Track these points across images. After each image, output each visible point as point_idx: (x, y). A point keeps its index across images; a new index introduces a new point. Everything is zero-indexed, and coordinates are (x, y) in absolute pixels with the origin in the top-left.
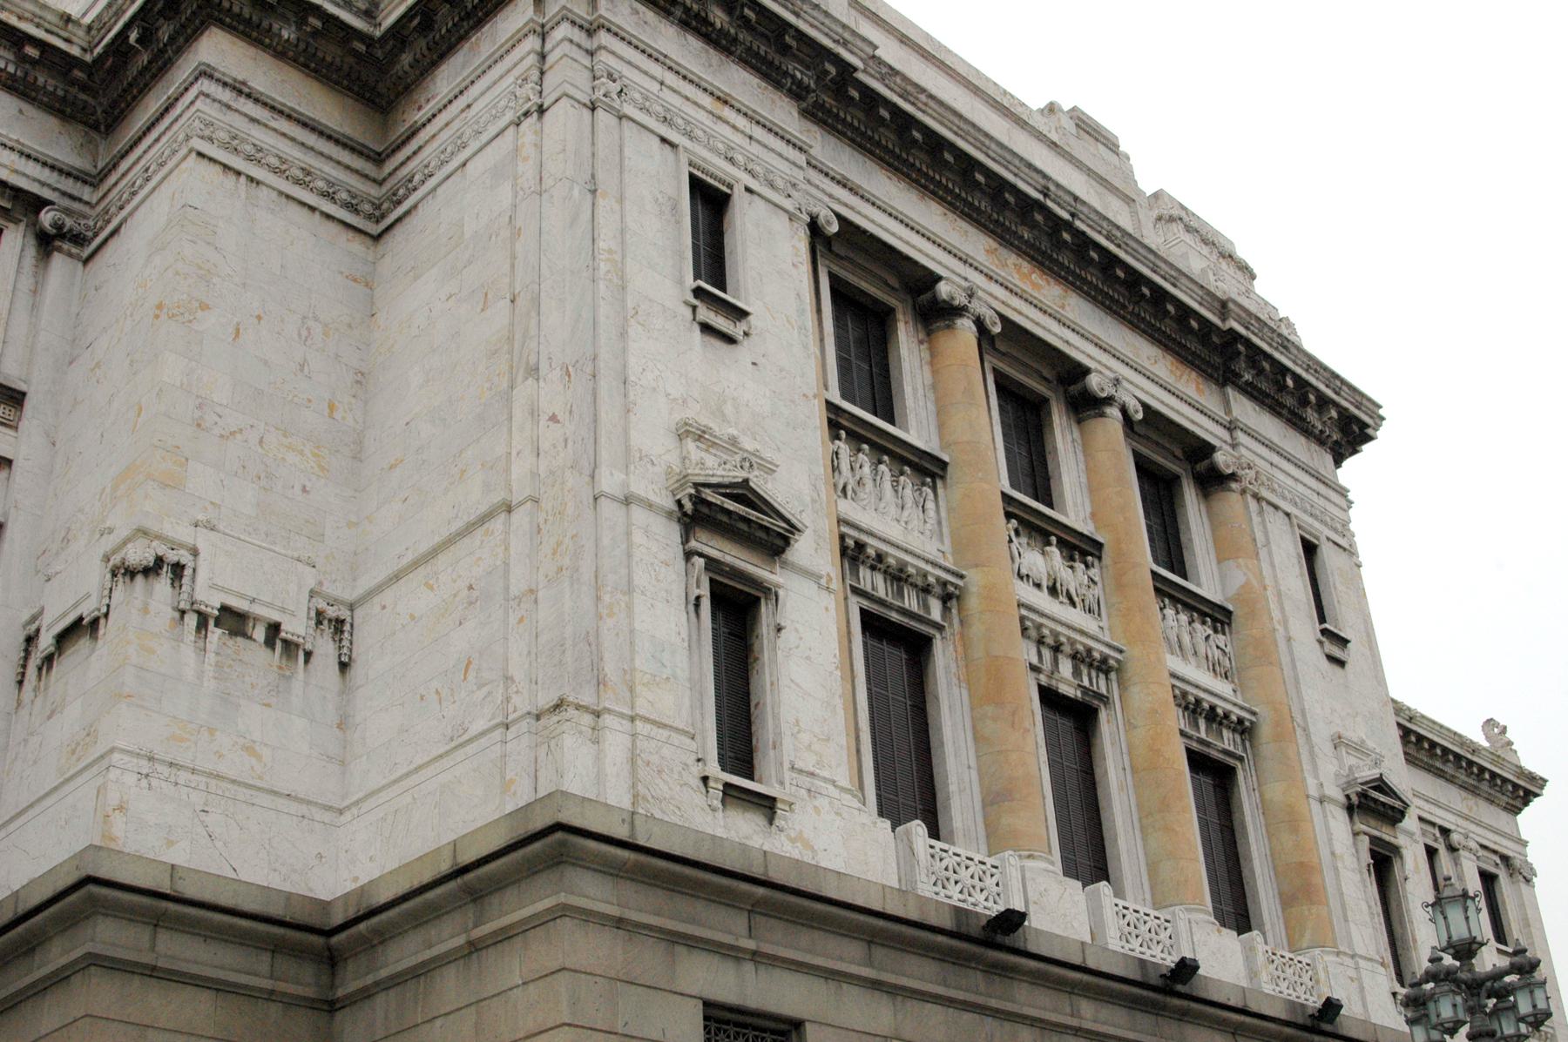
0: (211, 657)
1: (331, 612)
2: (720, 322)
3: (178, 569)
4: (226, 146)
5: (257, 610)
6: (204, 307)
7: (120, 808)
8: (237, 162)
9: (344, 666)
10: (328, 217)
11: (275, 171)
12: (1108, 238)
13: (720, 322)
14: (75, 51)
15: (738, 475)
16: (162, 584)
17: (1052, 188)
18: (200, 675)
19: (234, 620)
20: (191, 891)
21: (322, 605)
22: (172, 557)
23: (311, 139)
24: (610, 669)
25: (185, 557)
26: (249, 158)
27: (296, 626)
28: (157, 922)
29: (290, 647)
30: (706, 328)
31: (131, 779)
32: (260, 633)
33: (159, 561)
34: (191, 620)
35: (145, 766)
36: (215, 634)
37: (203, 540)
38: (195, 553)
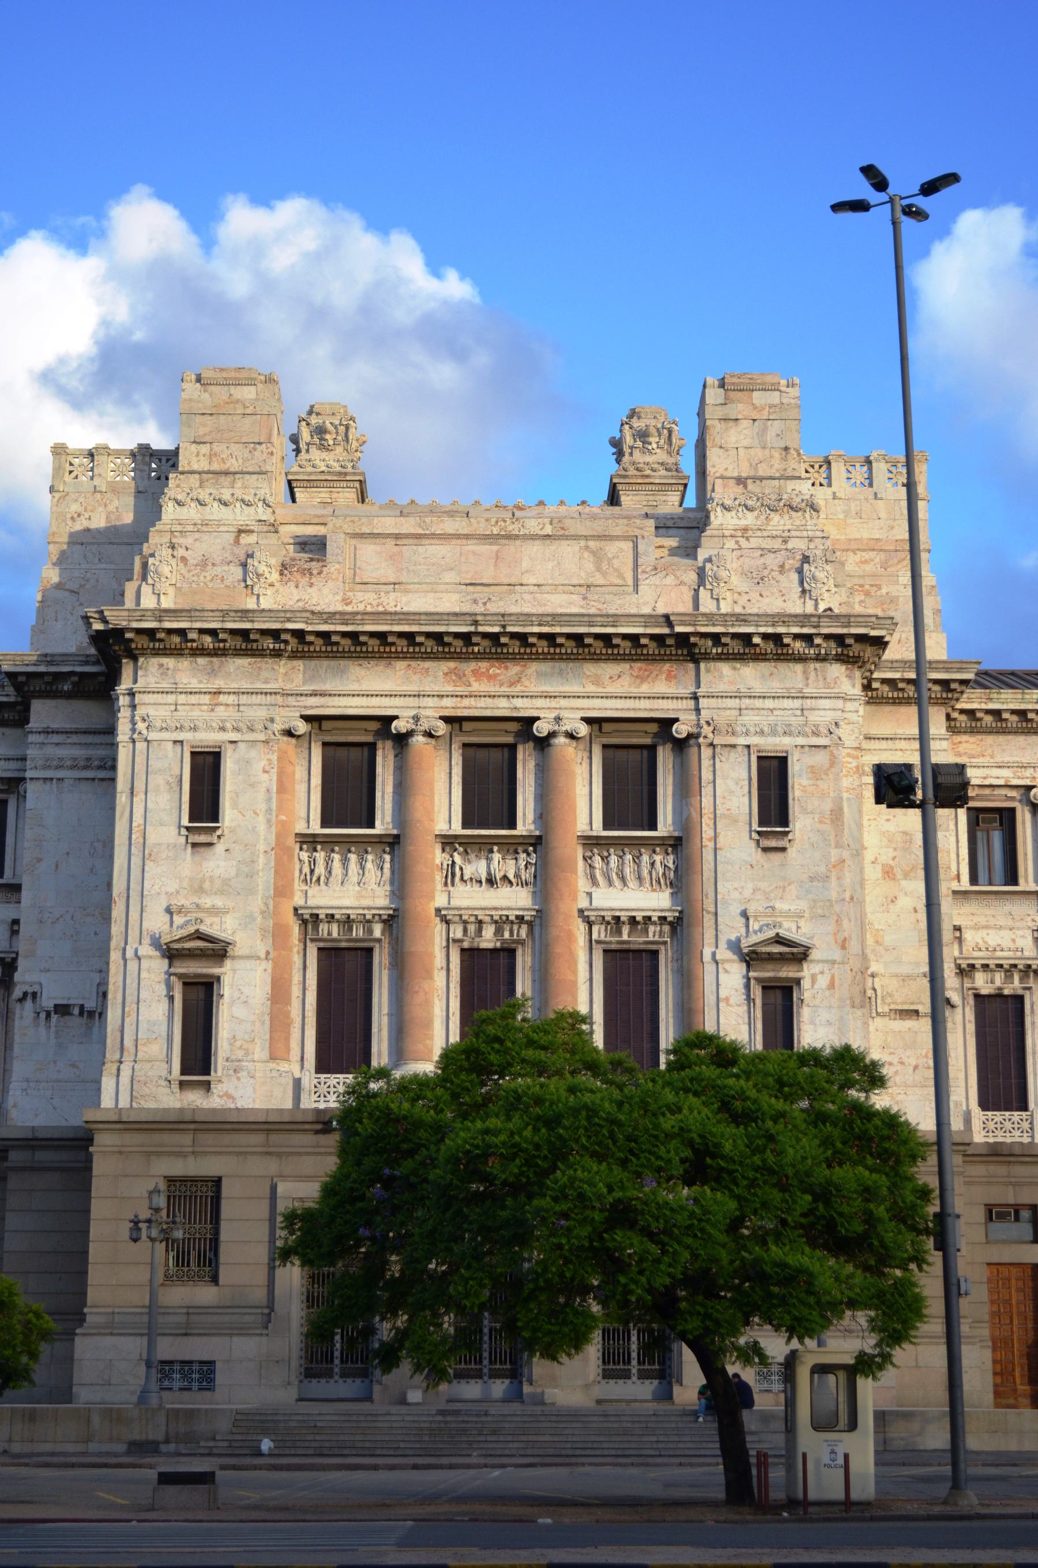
0: (53, 1029)
2: (202, 838)
3: (34, 995)
4: (46, 767)
5: (71, 1002)
6: (39, 860)
7: (15, 1106)
10: (102, 780)
11: (73, 767)
12: (540, 625)
13: (202, 838)
14: (12, 699)
15: (192, 929)
16: (29, 1004)
17: (479, 618)
18: (48, 1039)
19: (63, 1010)
20: (40, 1135)
22: (30, 990)
23: (90, 739)
24: (128, 1043)
25: (36, 988)
26: (57, 768)
28: (33, 1148)
29: (91, 1014)
30: (194, 845)
31: (18, 1093)
32: (76, 1011)
33: (25, 994)
34: (43, 1015)
35: (25, 1085)
36: (54, 1018)
37: (43, 978)
38: (41, 984)
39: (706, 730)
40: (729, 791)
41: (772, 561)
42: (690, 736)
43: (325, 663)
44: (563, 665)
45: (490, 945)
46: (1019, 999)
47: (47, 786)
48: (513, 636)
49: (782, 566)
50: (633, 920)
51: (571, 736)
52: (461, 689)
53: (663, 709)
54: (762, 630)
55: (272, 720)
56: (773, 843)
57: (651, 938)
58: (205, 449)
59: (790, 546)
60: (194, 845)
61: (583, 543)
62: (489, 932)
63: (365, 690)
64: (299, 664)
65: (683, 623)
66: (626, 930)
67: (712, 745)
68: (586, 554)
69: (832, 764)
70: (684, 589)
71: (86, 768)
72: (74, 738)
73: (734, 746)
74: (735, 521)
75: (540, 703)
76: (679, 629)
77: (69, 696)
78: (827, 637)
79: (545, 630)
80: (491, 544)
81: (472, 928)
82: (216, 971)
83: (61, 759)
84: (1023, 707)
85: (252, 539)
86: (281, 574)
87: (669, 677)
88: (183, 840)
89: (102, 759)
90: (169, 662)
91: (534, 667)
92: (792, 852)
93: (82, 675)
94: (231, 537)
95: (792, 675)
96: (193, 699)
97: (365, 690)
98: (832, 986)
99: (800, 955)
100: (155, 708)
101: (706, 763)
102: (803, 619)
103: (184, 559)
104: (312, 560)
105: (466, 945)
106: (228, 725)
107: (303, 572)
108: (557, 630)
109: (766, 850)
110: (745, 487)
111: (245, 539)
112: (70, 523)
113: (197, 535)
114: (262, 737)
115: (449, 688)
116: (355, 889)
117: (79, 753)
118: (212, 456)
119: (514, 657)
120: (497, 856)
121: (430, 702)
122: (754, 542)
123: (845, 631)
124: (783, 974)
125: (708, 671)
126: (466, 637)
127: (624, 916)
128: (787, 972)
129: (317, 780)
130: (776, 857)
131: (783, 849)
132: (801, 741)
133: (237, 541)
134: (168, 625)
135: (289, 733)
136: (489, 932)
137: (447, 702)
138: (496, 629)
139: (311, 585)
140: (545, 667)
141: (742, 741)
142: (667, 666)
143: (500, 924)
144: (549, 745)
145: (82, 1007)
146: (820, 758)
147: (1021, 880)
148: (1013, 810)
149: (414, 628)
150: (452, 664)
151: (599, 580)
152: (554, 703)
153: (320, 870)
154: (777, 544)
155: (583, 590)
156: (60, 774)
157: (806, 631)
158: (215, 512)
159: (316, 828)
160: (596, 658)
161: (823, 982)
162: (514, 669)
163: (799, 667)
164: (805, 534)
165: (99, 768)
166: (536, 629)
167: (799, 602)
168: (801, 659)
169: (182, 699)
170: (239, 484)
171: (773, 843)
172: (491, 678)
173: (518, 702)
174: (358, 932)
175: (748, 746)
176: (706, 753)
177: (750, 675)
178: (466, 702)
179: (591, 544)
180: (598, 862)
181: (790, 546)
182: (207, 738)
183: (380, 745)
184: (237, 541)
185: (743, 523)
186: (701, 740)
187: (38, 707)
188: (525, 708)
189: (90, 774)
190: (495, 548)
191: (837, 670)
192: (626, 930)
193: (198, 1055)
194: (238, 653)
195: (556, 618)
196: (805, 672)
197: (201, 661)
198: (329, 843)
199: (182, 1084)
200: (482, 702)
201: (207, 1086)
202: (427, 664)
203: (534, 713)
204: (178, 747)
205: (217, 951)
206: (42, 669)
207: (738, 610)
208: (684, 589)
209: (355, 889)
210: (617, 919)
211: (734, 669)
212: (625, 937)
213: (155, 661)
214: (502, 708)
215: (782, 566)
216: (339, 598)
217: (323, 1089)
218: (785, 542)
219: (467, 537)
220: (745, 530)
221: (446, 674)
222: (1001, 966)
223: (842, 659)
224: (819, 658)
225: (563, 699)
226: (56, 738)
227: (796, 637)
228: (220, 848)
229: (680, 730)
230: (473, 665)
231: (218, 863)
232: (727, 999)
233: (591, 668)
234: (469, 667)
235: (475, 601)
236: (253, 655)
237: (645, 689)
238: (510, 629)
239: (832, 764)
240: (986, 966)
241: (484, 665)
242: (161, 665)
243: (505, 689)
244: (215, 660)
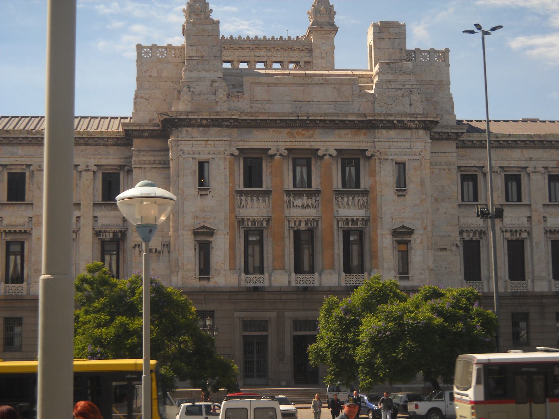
1: (166, 244)
2: (204, 193)
3: (139, 245)
4: (139, 164)
8: (140, 166)
9: (169, 252)
10: (160, 168)
11: (149, 164)
13: (204, 193)
16: (137, 249)
21: (163, 243)
22: (137, 244)
23: (155, 153)
24: (180, 264)
27: (159, 248)
29: (159, 252)
30: (201, 195)
32: (154, 251)
33: (136, 245)
39: (377, 154)
40: (386, 175)
41: (400, 93)
42: (372, 155)
43: (245, 129)
44: (328, 130)
45: (304, 229)
46: (478, 242)
47: (140, 171)
48: (311, 120)
49: (403, 95)
50: (352, 220)
51: (330, 155)
52: (292, 140)
53: (363, 146)
54: (397, 119)
55: (226, 150)
56: (401, 193)
57: (359, 226)
58: (194, 48)
59: (406, 87)
60: (201, 195)
61: (333, 86)
62: (303, 224)
63: (258, 140)
64: (235, 130)
65: (370, 116)
66: (350, 223)
67: (379, 159)
68: (335, 90)
69: (421, 166)
70: (369, 103)
71: (154, 164)
72: (149, 153)
73: (387, 159)
74: (386, 78)
75: (320, 144)
76: (369, 118)
77: (147, 137)
78: (419, 121)
79: (322, 118)
80: (302, 86)
81: (297, 223)
82: (210, 239)
83: (144, 161)
84: (481, 139)
85: (217, 84)
86: (228, 97)
87: (365, 134)
88: (197, 193)
89: (159, 161)
90: (190, 129)
91: (317, 131)
92: (407, 196)
93: (152, 130)
94: (209, 84)
95: (408, 133)
96: (199, 143)
97: (258, 140)
98: (421, 242)
99: (411, 232)
100: (186, 146)
101: (377, 165)
102: (412, 115)
103: (193, 92)
104: (238, 92)
105: (295, 229)
106: (211, 152)
107: (235, 97)
108: (326, 118)
109: (399, 196)
110: (389, 65)
111: (215, 84)
112: (144, 73)
113: (197, 83)
114: (223, 156)
115: (289, 139)
116: (255, 210)
117: (152, 158)
118: (197, 51)
119: (311, 128)
120: (305, 198)
121: (281, 143)
122: (393, 86)
123: (426, 119)
124: (405, 239)
125: (378, 132)
126: (295, 121)
127: (350, 218)
128: (406, 238)
129: (242, 171)
130: (402, 198)
131: (404, 195)
132: (410, 157)
133: (212, 85)
134: (190, 117)
135: (232, 155)
136: (303, 224)
137: (288, 143)
138: (305, 118)
139: (239, 101)
140: (321, 131)
141: (390, 157)
142: (364, 131)
143: (307, 222)
144: (323, 159)
145: (156, 249)
146: (417, 163)
147: (479, 200)
148: (477, 175)
149: (277, 118)
150: (289, 130)
151: (339, 99)
152: (325, 144)
153: (244, 203)
154: (401, 87)
155: (334, 103)
156: (144, 166)
157: (412, 119)
158: (204, 74)
159: (242, 188)
160: (339, 128)
161: (418, 241)
162: (311, 132)
163: (409, 131)
164: (410, 83)
165: (159, 164)
166: (319, 118)
167: (409, 108)
168: (410, 128)
169: (195, 143)
170: (211, 64)
171: (401, 193)
172: (303, 135)
173: (312, 144)
174: (258, 225)
175: (392, 159)
176: (378, 161)
177: (393, 133)
178: (294, 143)
179: (337, 86)
180: (340, 199)
181: (406, 87)
182: (204, 157)
183: (264, 159)
184: (212, 85)
185: (389, 78)
186: (376, 157)
187: (136, 142)
188: (315, 146)
189: (155, 166)
190: (303, 88)
191: (422, 132)
192: (350, 223)
193: (205, 269)
194: (214, 126)
195: (326, 114)
196: (411, 133)
197: (201, 129)
198: (247, 193)
199: (200, 279)
200: (300, 144)
201: (208, 279)
202: (281, 130)
203: (318, 148)
204: (194, 160)
205: (211, 233)
206: (138, 128)
207: (388, 112)
208: (369, 103)
209: (255, 210)
210: (347, 219)
211: (387, 132)
212: (350, 226)
213: (184, 129)
214: (307, 146)
215: (403, 95)
216: (248, 106)
217: (248, 280)
218: (404, 86)
219: (293, 84)
220: (390, 81)
221: (287, 133)
222: (472, 230)
223: (423, 128)
224: (416, 128)
225: (329, 143)
226: (142, 153)
227: (409, 121)
228: (210, 196)
229: (368, 154)
230: (296, 130)
231: (209, 201)
232: (386, 248)
233: (337, 132)
234: (295, 131)
235: (296, 107)
236: (219, 127)
237: (356, 139)
238: (310, 118)
239: (421, 166)
240: (467, 231)
241: (300, 130)
242: (187, 131)
243: (309, 140)
244: (206, 128)
